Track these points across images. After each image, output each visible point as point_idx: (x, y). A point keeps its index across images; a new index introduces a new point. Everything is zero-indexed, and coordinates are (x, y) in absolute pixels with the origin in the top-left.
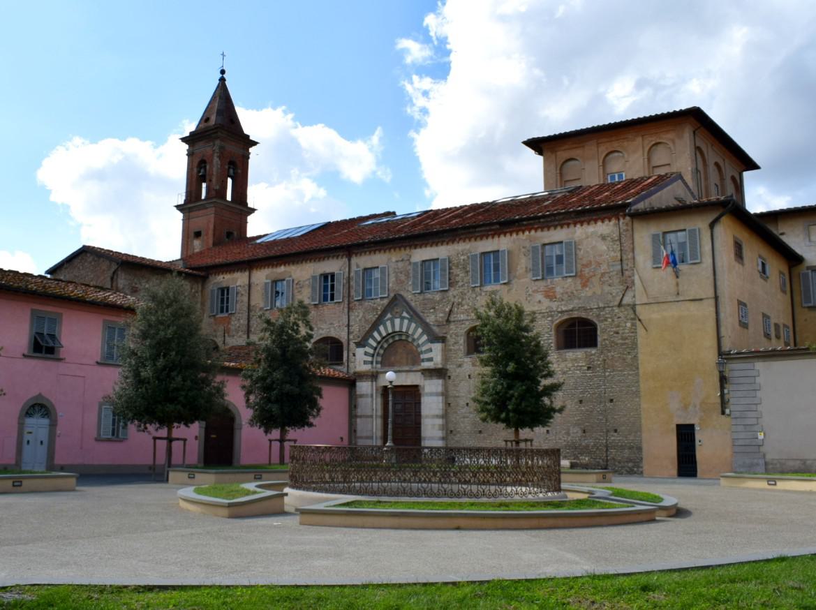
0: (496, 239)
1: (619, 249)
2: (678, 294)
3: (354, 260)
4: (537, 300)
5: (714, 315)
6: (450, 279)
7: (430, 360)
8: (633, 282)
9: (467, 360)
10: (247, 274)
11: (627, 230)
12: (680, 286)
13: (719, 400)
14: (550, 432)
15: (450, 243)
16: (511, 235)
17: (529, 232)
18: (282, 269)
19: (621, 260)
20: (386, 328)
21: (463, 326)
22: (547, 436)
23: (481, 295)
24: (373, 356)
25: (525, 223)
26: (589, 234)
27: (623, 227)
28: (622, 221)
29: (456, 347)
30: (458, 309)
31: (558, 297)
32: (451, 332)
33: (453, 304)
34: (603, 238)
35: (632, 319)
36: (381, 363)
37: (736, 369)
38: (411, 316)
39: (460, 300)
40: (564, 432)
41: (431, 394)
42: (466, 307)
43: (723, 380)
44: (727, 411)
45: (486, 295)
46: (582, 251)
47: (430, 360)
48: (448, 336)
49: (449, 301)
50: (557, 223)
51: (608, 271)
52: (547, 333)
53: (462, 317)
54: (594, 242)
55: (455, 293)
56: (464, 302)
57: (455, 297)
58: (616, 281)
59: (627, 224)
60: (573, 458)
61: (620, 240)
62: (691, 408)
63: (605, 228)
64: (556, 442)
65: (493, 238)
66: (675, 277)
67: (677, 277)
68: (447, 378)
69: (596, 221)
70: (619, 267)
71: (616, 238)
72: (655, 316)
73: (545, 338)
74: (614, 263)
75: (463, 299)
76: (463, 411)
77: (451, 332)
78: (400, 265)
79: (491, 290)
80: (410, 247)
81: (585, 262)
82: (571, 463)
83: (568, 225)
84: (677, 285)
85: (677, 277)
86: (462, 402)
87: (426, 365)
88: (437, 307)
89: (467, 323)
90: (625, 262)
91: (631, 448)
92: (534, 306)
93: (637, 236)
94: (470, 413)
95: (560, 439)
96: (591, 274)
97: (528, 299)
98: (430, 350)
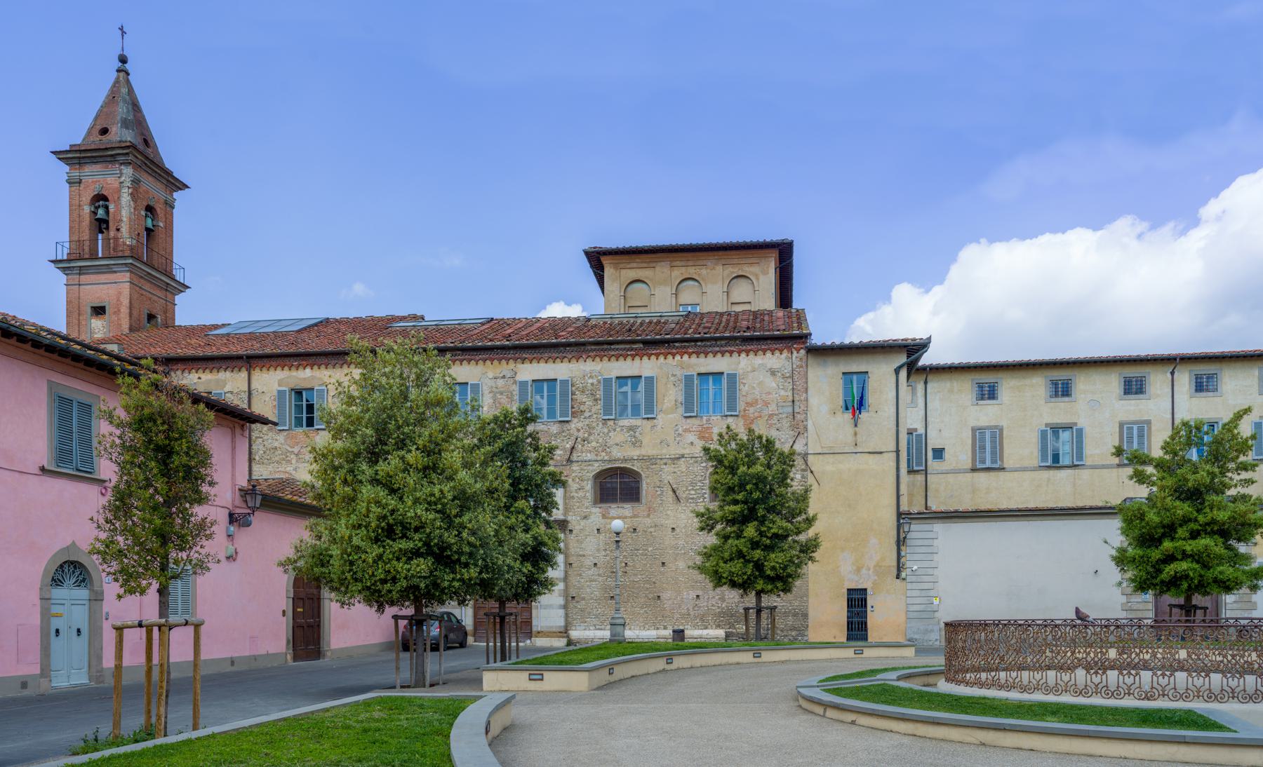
1: (791, 387)
2: (856, 445)
4: (689, 442)
5: (895, 470)
6: (573, 407)
8: (806, 428)
9: (596, 510)
10: (244, 374)
11: (802, 367)
12: (858, 436)
13: (895, 563)
15: (574, 361)
18: (308, 372)
19: (793, 401)
21: (590, 468)
23: (615, 430)
25: (677, 344)
26: (756, 366)
27: (796, 362)
29: (581, 494)
30: (583, 446)
32: (573, 475)
33: (577, 439)
35: (803, 470)
37: (917, 531)
39: (586, 435)
40: (717, 597)
42: (594, 444)
43: (900, 542)
44: (903, 575)
45: (622, 430)
46: (747, 386)
48: (570, 480)
49: (571, 435)
50: (718, 349)
51: (777, 412)
53: (589, 456)
54: (762, 377)
55: (580, 425)
56: (592, 438)
57: (578, 430)
58: (786, 424)
60: (728, 626)
61: (792, 377)
62: (864, 571)
63: (777, 360)
64: (708, 609)
66: (853, 426)
67: (856, 426)
68: (568, 532)
69: (764, 352)
70: (790, 410)
71: (788, 375)
72: (829, 468)
73: (698, 487)
74: (784, 404)
75: (590, 434)
76: (591, 572)
77: (573, 475)
78: (501, 382)
79: (628, 424)
80: (515, 360)
81: (749, 400)
82: (726, 632)
83: (731, 353)
84: (856, 434)
85: (856, 426)
86: (588, 562)
89: (596, 465)
90: (797, 403)
91: (795, 615)
92: (685, 448)
93: (810, 375)
94: (599, 575)
96: (756, 414)
97: (677, 439)
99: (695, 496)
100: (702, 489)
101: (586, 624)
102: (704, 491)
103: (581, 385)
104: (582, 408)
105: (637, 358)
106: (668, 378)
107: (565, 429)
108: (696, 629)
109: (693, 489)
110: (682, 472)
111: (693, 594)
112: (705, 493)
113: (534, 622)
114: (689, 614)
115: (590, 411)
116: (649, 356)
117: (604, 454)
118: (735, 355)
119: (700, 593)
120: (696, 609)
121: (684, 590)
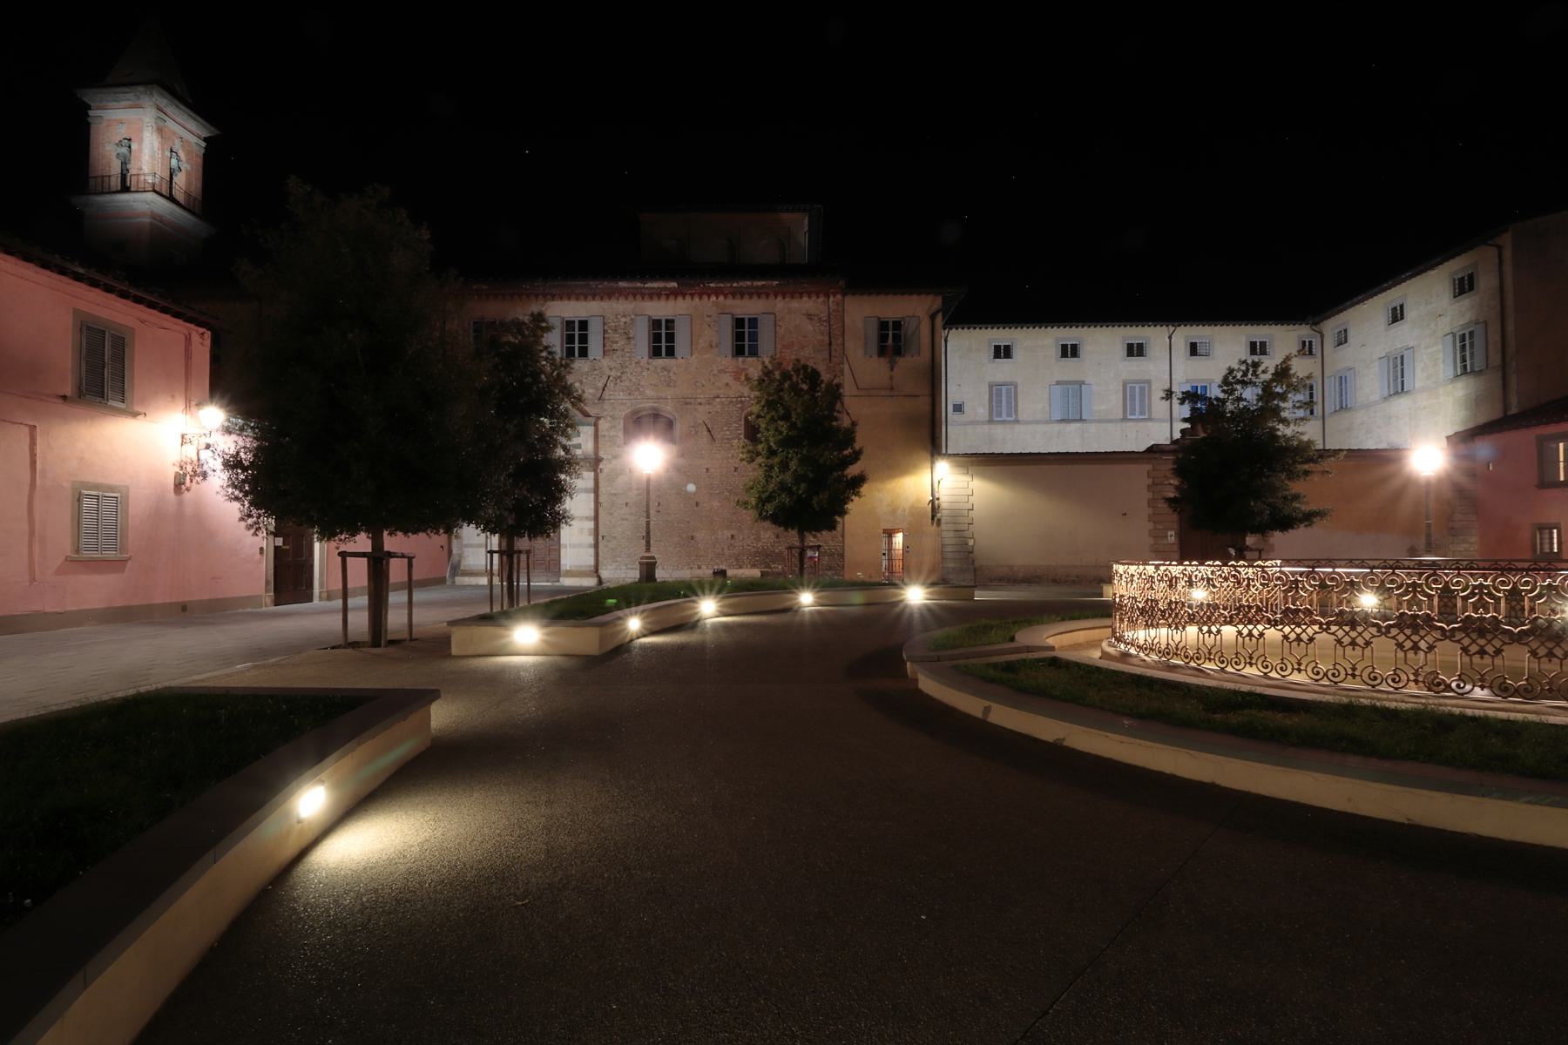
0: (671, 302)
11: (838, 311)
28: (831, 299)
34: (809, 316)
46: (783, 328)
52: (735, 422)
55: (613, 364)
56: (624, 377)
59: (838, 304)
67: (892, 369)
71: (824, 319)
75: (622, 373)
80: (545, 296)
85: (892, 369)
88: (584, 381)
91: (832, 555)
95: (748, 545)
104: (615, 346)
105: (672, 297)
107: (597, 367)
110: (717, 412)
111: (728, 534)
113: (563, 562)
114: (724, 554)
115: (623, 350)
116: (684, 296)
117: (637, 393)
118: (773, 297)
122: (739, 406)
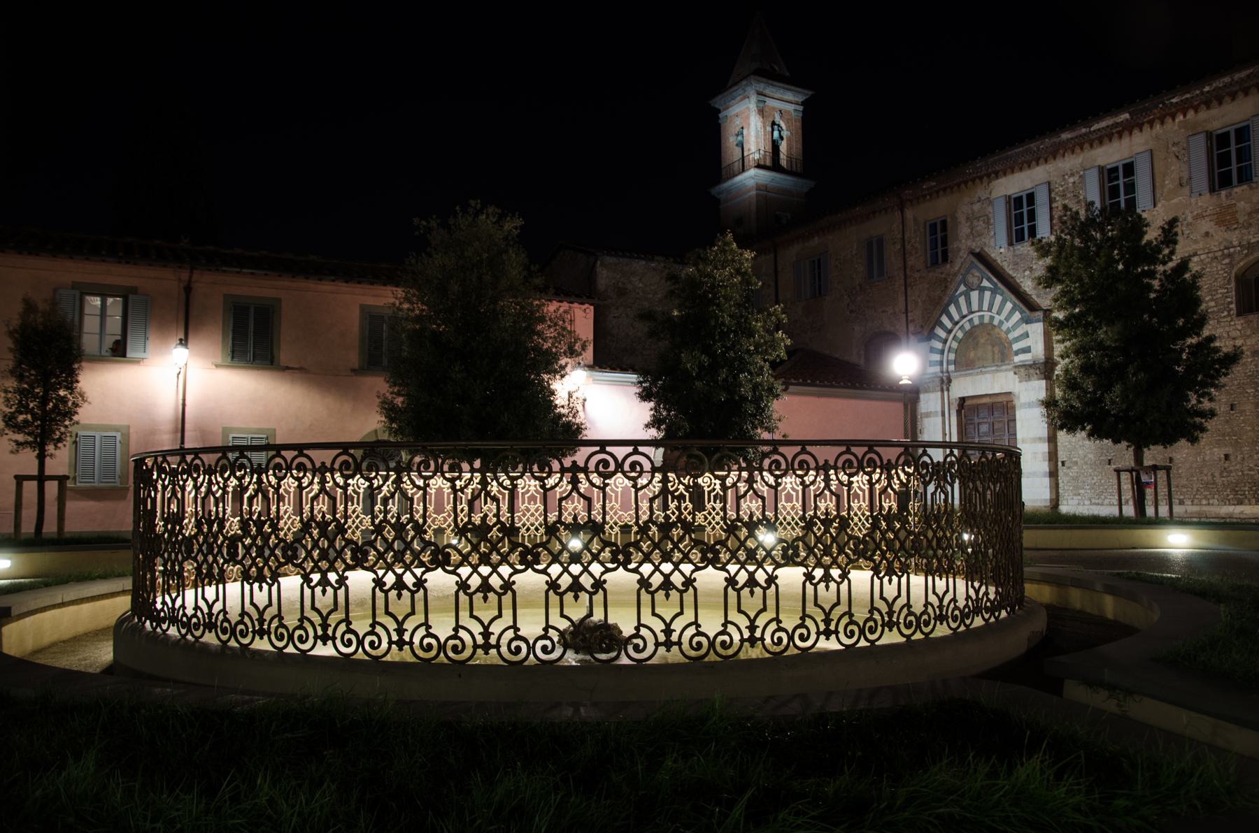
0: (1126, 140)
3: (909, 214)
7: (1027, 350)
14: (1232, 458)
16: (1151, 127)
17: (1185, 116)
20: (958, 308)
22: (1226, 465)
24: (942, 352)
31: (1241, 221)
36: (955, 362)
38: (995, 285)
41: (1030, 405)
47: (1027, 350)
64: (1243, 474)
65: (1120, 137)
87: (1018, 359)
88: (1034, 267)
95: (1251, 469)
98: (1026, 335)
99: (1215, 309)
100: (1227, 297)
101: (1079, 497)
102: (1229, 300)
103: (1061, 189)
106: (1168, 148)
108: (1225, 505)
109: (1212, 300)
112: (1231, 303)
114: (1214, 483)
119: (1229, 450)
120: (1225, 474)
121: (1207, 448)
122: (1227, 261)
